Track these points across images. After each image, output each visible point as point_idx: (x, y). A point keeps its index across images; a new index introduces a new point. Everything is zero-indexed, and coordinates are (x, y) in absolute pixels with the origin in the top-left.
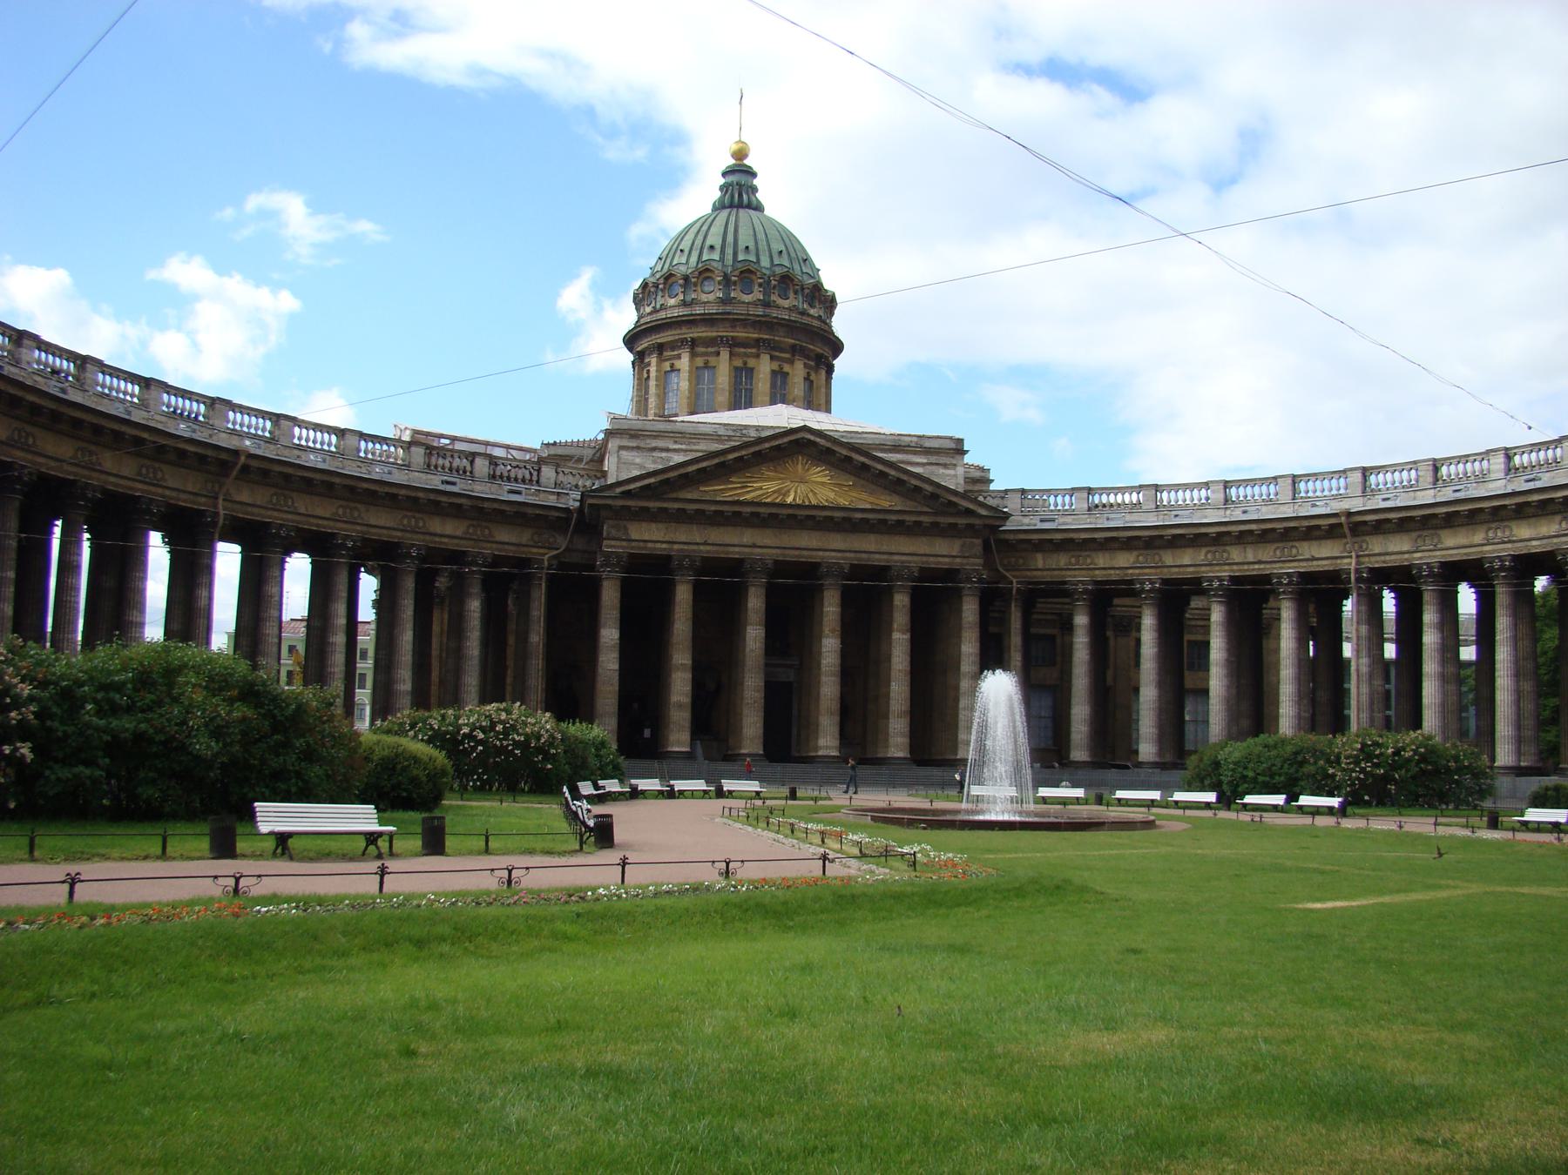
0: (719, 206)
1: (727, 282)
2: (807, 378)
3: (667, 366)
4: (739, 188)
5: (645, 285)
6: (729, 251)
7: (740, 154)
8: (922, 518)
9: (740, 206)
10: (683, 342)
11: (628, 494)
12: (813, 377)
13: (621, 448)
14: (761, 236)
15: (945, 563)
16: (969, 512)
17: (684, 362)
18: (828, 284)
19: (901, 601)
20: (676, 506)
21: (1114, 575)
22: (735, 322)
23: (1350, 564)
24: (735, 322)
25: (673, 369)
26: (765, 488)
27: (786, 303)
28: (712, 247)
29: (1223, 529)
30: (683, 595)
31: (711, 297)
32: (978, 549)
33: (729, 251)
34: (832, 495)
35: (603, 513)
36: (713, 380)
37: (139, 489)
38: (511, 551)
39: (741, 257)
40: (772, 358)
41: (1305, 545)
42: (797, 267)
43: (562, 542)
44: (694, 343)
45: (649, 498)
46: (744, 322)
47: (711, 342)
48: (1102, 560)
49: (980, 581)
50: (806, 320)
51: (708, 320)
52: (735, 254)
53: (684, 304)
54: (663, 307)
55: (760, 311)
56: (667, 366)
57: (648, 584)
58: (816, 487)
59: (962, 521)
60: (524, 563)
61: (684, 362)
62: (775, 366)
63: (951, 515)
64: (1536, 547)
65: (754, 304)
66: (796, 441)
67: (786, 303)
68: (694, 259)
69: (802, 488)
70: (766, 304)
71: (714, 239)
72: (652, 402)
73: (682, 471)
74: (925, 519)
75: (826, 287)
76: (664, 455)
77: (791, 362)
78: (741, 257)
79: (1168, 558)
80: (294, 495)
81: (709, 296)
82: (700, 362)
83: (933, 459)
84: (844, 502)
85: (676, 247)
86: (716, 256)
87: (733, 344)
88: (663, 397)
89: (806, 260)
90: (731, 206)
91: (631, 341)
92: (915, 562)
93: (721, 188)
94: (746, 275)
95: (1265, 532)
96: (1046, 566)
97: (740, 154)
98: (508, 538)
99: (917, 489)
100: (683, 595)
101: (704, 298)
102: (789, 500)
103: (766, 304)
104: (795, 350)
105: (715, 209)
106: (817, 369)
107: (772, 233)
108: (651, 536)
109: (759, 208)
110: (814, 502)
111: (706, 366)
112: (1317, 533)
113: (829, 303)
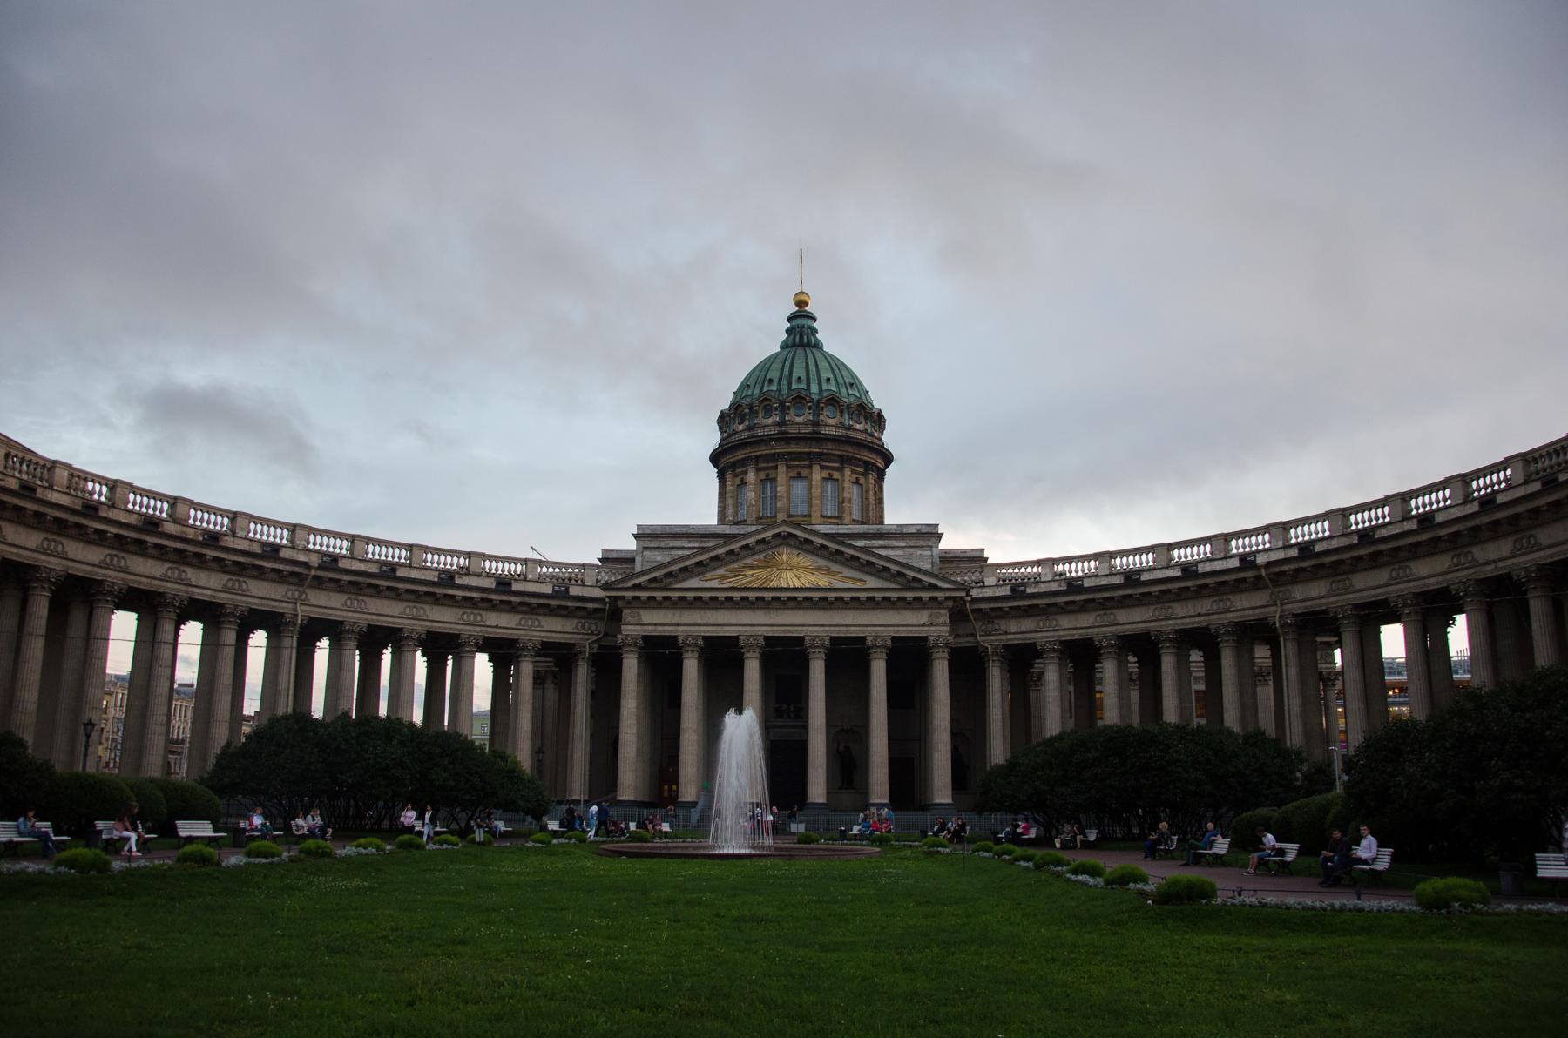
2: (857, 482)
3: (738, 480)
4: (801, 332)
5: (723, 416)
6: (785, 382)
7: (801, 304)
8: (887, 594)
9: (802, 345)
11: (638, 587)
12: (862, 480)
13: (645, 548)
14: (812, 367)
16: (932, 587)
17: (751, 477)
18: (878, 402)
19: (879, 668)
20: (678, 594)
21: (1077, 635)
23: (1275, 614)
25: (743, 483)
26: (752, 577)
27: (832, 422)
28: (771, 381)
29: (1164, 587)
30: (691, 668)
31: (770, 421)
32: (944, 617)
33: (785, 382)
34: (813, 579)
35: (620, 603)
36: (774, 490)
37: (223, 597)
38: (558, 638)
39: (794, 386)
40: (822, 468)
41: (1238, 596)
42: (843, 391)
43: (601, 627)
45: (654, 589)
46: (798, 439)
47: (773, 458)
48: (1065, 622)
49: (947, 644)
50: (851, 434)
52: (790, 384)
53: (750, 428)
54: (735, 433)
55: (810, 429)
56: (738, 480)
57: (662, 657)
58: (796, 573)
59: (925, 595)
60: (570, 646)
62: (825, 474)
63: (914, 589)
64: (1434, 583)
65: (805, 424)
66: (779, 535)
67: (832, 422)
68: (757, 391)
69: (789, 574)
70: (816, 424)
71: (774, 374)
72: (730, 510)
73: (682, 565)
74: (894, 595)
75: (876, 405)
76: (681, 553)
77: (841, 470)
78: (794, 386)
79: (1122, 616)
80: (367, 599)
81: (767, 423)
82: (762, 475)
83: (911, 543)
84: (823, 582)
85: (745, 385)
86: (774, 388)
88: (736, 505)
89: (854, 383)
90: (794, 345)
91: (715, 458)
93: (788, 331)
94: (800, 399)
95: (1201, 587)
96: (1018, 630)
97: (801, 304)
98: (555, 628)
99: (885, 569)
100: (691, 668)
101: (765, 421)
102: (774, 584)
103: (816, 424)
104: (844, 461)
105: (782, 347)
106: (866, 474)
107: (823, 364)
108: (657, 621)
109: (817, 346)
110: (798, 584)
111: (768, 479)
112: (1243, 586)
113: (878, 420)
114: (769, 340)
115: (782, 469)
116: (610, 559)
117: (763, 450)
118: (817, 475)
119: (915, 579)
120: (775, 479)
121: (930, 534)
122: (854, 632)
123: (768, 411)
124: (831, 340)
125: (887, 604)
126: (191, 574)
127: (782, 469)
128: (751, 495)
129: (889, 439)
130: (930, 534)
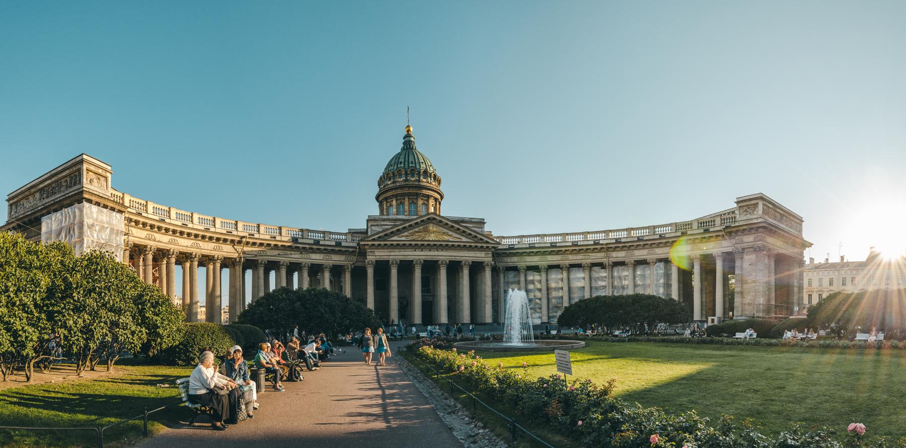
0: (403, 149)
1: (406, 174)
4: (408, 145)
7: (408, 135)
10: (393, 196)
15: (480, 260)
16: (487, 242)
17: (394, 203)
22: (409, 187)
24: (409, 187)
25: (391, 205)
36: (404, 208)
44: (396, 196)
51: (401, 187)
53: (393, 183)
59: (485, 245)
61: (394, 203)
65: (416, 181)
70: (419, 181)
71: (402, 160)
74: (473, 245)
77: (428, 201)
85: (389, 165)
87: (409, 195)
92: (471, 260)
97: (408, 135)
114: (398, 147)
115: (407, 199)
116: (353, 233)
117: (399, 191)
118: (420, 202)
119: (481, 239)
120: (403, 204)
121: (481, 223)
122: (458, 259)
123: (400, 176)
124: (420, 147)
125: (470, 248)
126: (201, 244)
127: (407, 199)
128: (395, 210)
129: (442, 188)
130: (481, 223)
